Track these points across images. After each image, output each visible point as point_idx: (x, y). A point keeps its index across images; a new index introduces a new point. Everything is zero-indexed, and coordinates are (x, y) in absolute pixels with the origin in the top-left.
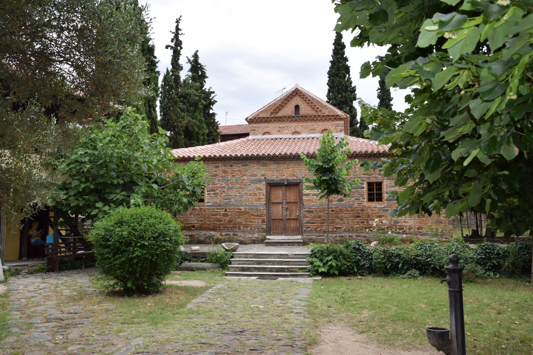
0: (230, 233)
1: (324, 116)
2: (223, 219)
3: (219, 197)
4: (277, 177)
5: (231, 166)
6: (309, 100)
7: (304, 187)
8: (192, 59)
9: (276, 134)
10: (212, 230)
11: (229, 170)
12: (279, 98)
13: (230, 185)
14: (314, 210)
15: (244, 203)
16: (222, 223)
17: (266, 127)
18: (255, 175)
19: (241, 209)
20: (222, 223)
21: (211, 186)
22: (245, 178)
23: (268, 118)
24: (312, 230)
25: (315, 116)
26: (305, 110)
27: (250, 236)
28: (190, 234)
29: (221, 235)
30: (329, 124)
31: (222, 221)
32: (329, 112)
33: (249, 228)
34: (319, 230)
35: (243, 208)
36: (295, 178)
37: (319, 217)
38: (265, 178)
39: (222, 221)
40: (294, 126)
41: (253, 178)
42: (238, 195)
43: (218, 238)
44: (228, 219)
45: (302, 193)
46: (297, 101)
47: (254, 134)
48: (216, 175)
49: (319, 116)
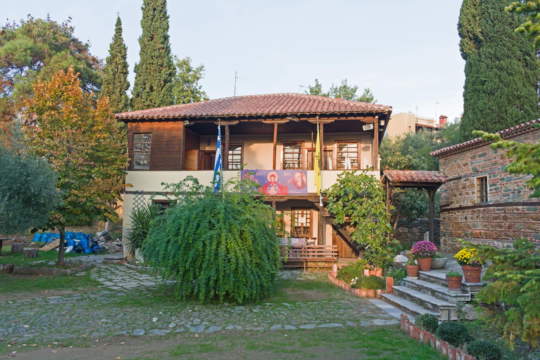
3: (499, 193)
10: (495, 239)
16: (503, 229)
19: (518, 210)
20: (503, 229)
21: (492, 178)
29: (503, 247)
42: (516, 188)
44: (508, 224)
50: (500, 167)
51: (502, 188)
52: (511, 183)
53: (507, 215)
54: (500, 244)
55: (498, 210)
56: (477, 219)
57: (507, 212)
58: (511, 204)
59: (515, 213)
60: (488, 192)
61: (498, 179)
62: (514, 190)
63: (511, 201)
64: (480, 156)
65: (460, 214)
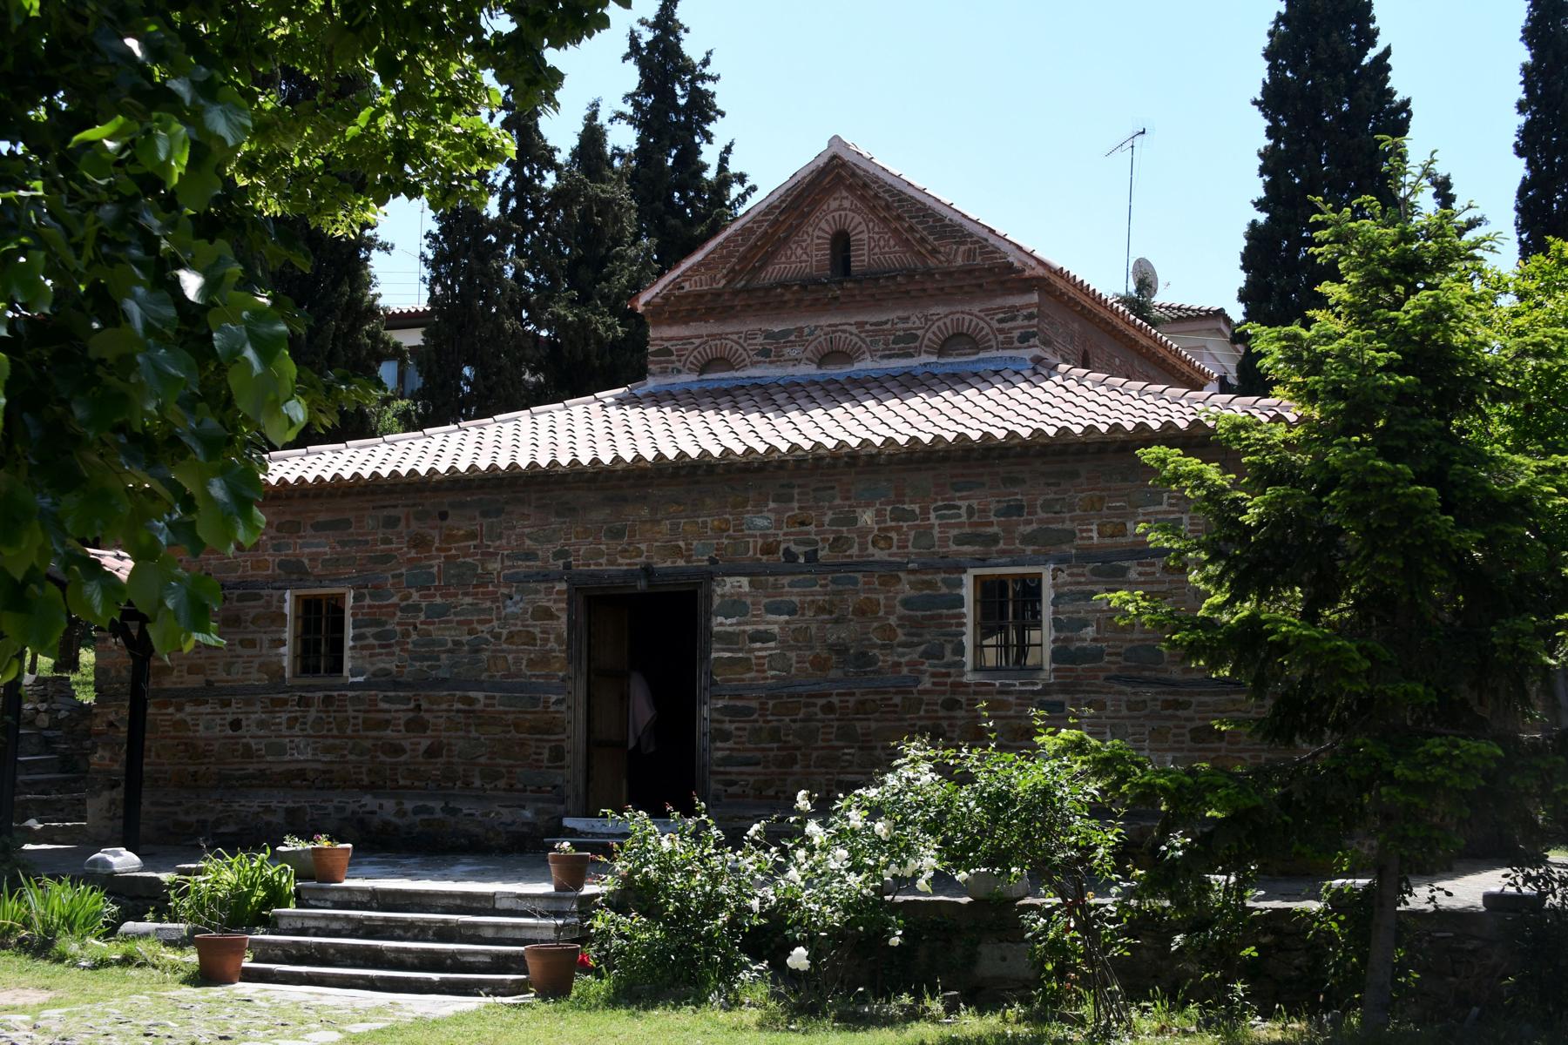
0: (431, 804)
1: (948, 274)
2: (406, 744)
3: (397, 649)
4: (611, 563)
5: (443, 516)
6: (888, 207)
7: (717, 601)
8: (647, 36)
9: (754, 364)
11: (435, 533)
12: (764, 205)
13: (438, 600)
14: (754, 704)
15: (484, 676)
17: (713, 336)
18: (530, 555)
20: (403, 758)
21: (367, 601)
22: (494, 566)
23: (717, 294)
24: (744, 795)
25: (910, 274)
26: (873, 247)
27: (506, 815)
28: (290, 804)
29: (401, 813)
30: (975, 310)
31: (404, 751)
32: (970, 254)
33: (502, 783)
34: (771, 792)
35: (480, 695)
36: (681, 563)
37: (775, 734)
38: (567, 566)
39: (404, 751)
40: (823, 325)
41: (523, 566)
43: (387, 823)
44: (425, 743)
45: (708, 628)
46: (839, 210)
47: (664, 372)
48: (386, 558)
49: (929, 273)
50: (403, 570)
51: (406, 634)
52: (448, 622)
53: (427, 716)
54: (389, 805)
55: (387, 699)
56: (290, 727)
57: (424, 706)
58: (440, 683)
59: (458, 711)
60: (348, 643)
61: (396, 605)
62: (455, 643)
63: (442, 674)
64: (319, 527)
65: (207, 709)
